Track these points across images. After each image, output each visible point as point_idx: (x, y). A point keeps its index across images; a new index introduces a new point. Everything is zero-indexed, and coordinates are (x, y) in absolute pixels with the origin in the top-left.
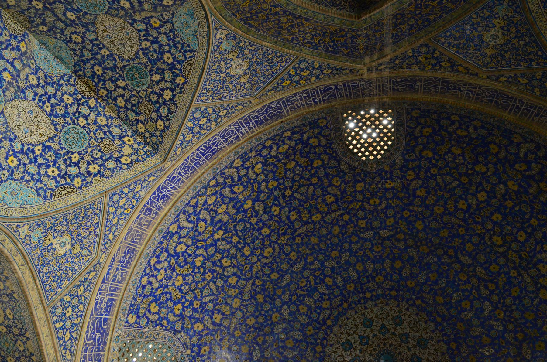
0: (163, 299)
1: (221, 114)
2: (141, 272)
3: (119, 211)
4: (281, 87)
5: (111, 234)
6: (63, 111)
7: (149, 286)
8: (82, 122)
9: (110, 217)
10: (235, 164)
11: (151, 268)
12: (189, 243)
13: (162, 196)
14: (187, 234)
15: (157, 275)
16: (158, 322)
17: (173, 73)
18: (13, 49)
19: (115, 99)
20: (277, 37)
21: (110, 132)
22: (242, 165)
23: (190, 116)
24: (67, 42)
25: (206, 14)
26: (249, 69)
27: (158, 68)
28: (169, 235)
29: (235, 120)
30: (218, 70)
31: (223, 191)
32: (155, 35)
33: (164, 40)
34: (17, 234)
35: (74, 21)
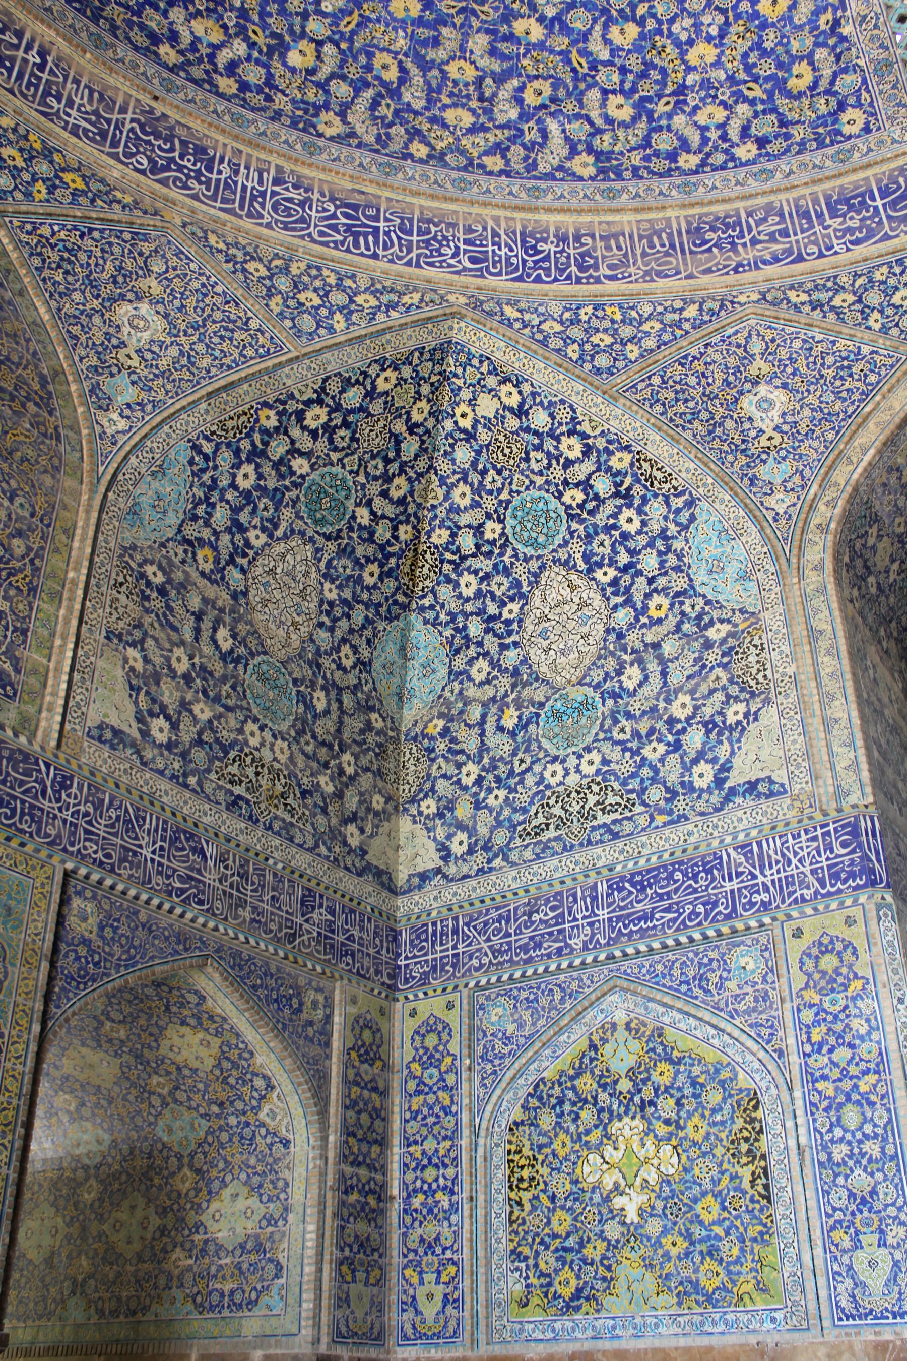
0: (766, 68)
1: (264, 272)
2: (729, 174)
3: (627, 331)
4: (95, 186)
5: (686, 314)
6: (497, 579)
7: (753, 131)
8: (492, 530)
10: (337, 128)
11: (708, 155)
12: (594, 95)
13: (534, 257)
14: (578, 117)
16: (831, 42)
17: (266, 444)
18: (454, 740)
19: (402, 501)
20: (10, 303)
21: (474, 464)
22: (326, 107)
23: (324, 338)
24: (364, 665)
25: (108, 490)
26: (122, 297)
27: (282, 477)
28: (608, 167)
29: (247, 224)
30: (184, 361)
31: (418, 105)
32: (225, 538)
33: (221, 516)
34: (794, 511)
35: (323, 688)
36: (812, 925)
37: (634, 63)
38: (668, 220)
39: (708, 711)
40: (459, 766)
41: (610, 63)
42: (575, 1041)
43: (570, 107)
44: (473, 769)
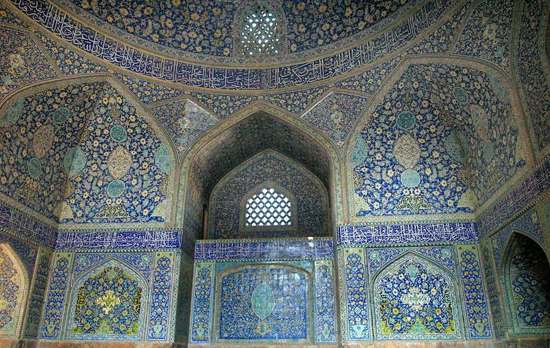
0: (210, 27)
1: (57, 51)
3: (154, 92)
4: (10, 16)
6: (105, 144)
8: (106, 132)
9: (159, 98)
14: (158, 22)
15: (194, 39)
18: (83, 185)
19: (82, 118)
21: (105, 114)
24: (61, 159)
26: (12, 52)
28: (162, 40)
29: (54, 34)
33: (30, 118)
36: (162, 254)
37: (177, 11)
38: (174, 62)
39: (151, 196)
40: (83, 192)
41: (170, 9)
42: (101, 269)
43: (156, 18)
44: (88, 195)
